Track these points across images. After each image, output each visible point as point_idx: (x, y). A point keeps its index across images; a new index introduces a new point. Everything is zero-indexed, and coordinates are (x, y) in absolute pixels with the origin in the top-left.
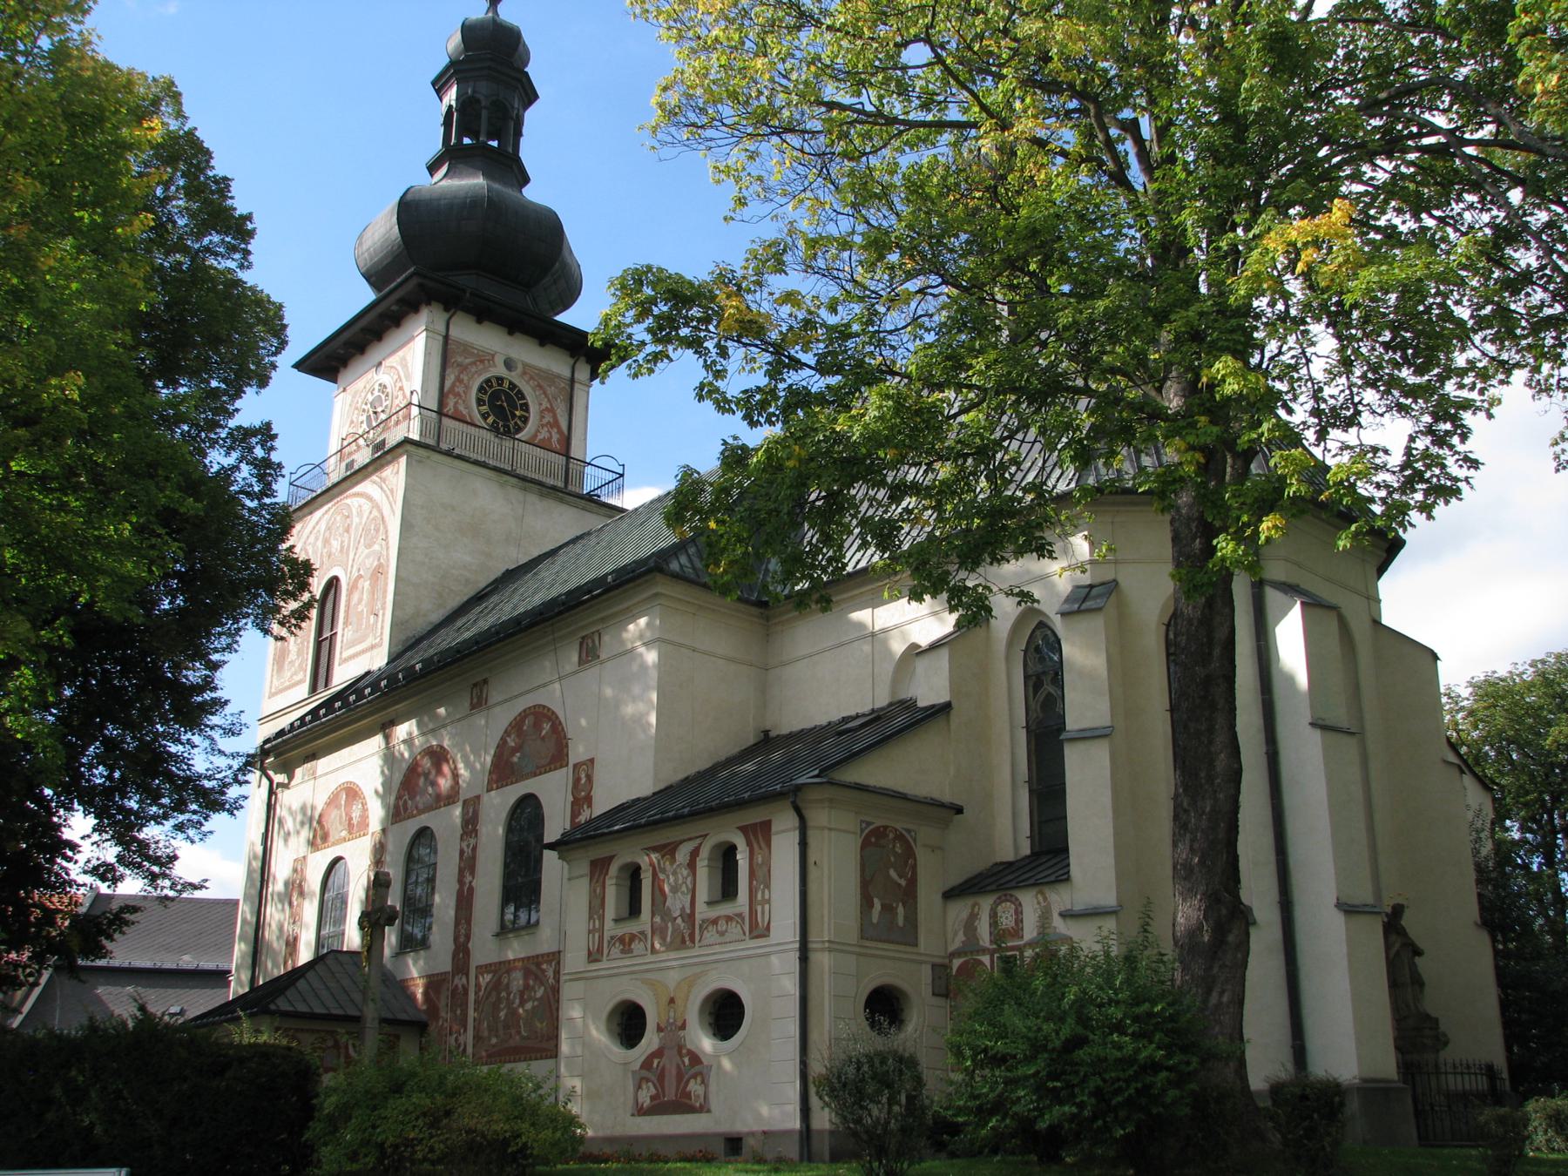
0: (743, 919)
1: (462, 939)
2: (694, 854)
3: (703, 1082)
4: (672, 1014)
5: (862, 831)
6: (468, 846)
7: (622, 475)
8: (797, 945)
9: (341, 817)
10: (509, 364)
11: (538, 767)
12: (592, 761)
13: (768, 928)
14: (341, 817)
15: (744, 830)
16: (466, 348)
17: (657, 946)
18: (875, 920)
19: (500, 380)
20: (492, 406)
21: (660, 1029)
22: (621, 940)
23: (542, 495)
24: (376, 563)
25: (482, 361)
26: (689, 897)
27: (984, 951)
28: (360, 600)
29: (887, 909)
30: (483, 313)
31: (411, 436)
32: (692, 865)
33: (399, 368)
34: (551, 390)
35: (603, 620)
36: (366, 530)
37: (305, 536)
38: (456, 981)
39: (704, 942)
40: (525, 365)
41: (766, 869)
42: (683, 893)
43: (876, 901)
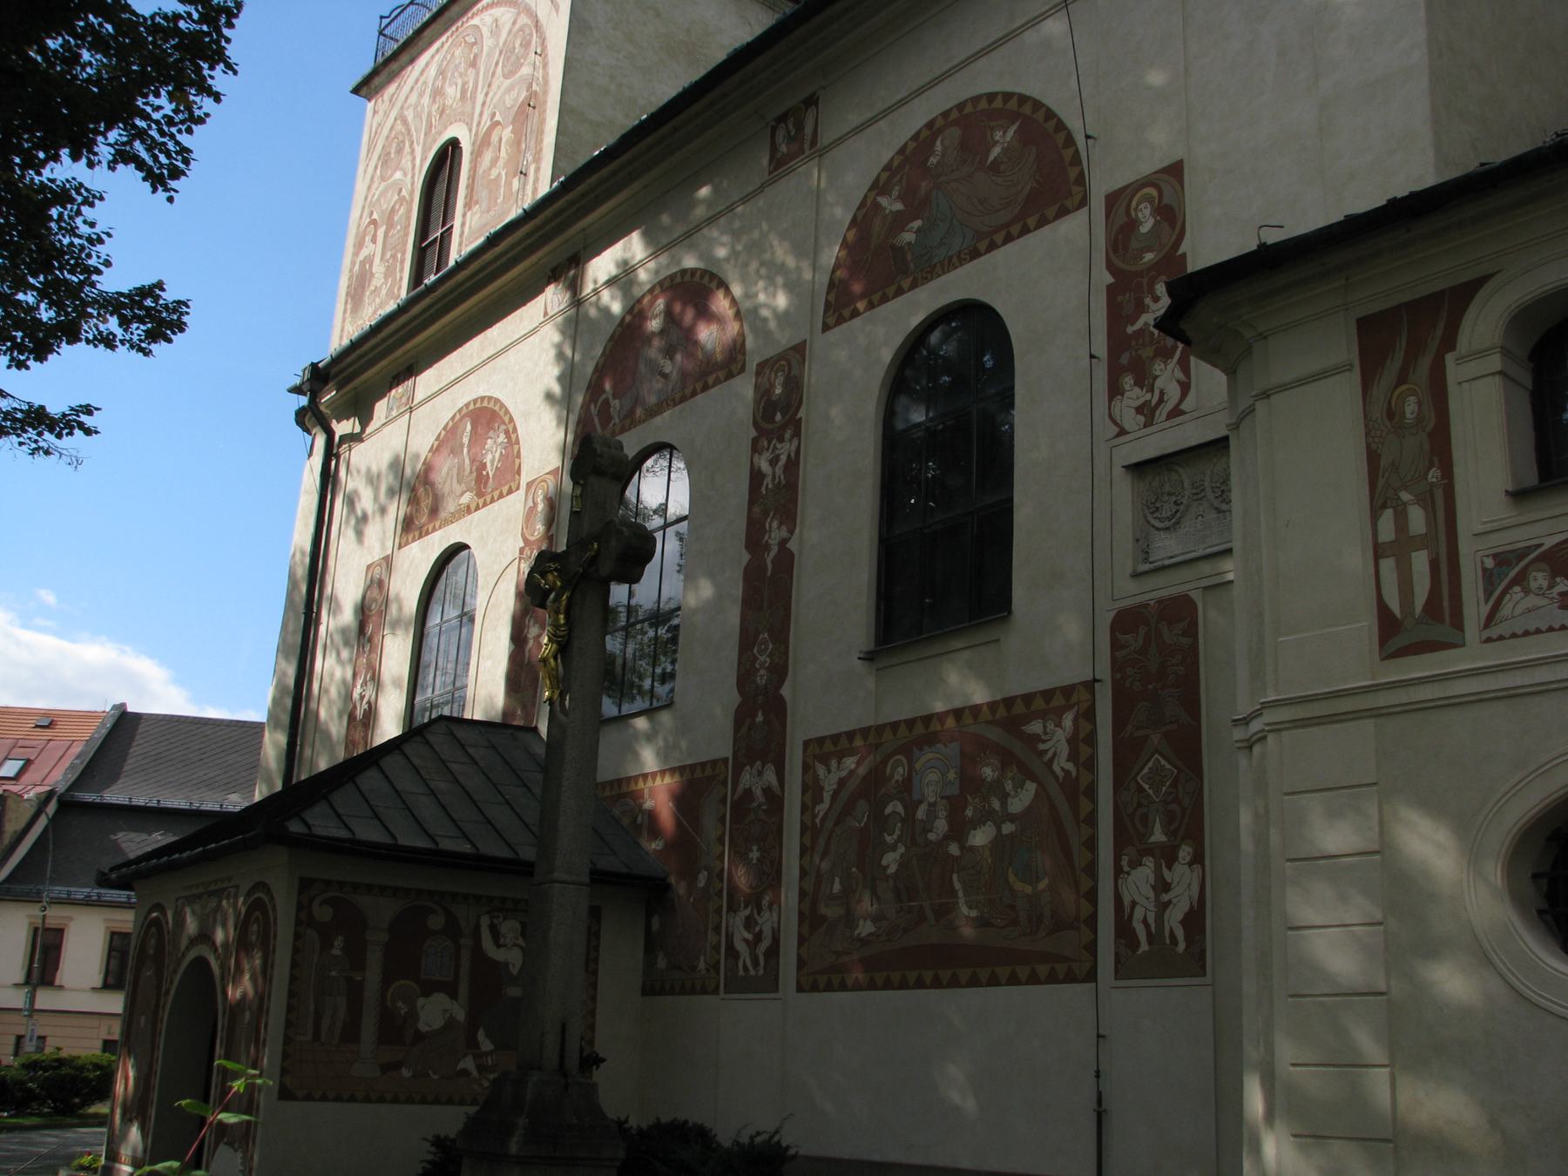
1: (762, 678)
6: (773, 462)
9: (461, 468)
14: (461, 468)
24: (524, 94)
36: (507, 51)
37: (402, 98)
38: (747, 778)
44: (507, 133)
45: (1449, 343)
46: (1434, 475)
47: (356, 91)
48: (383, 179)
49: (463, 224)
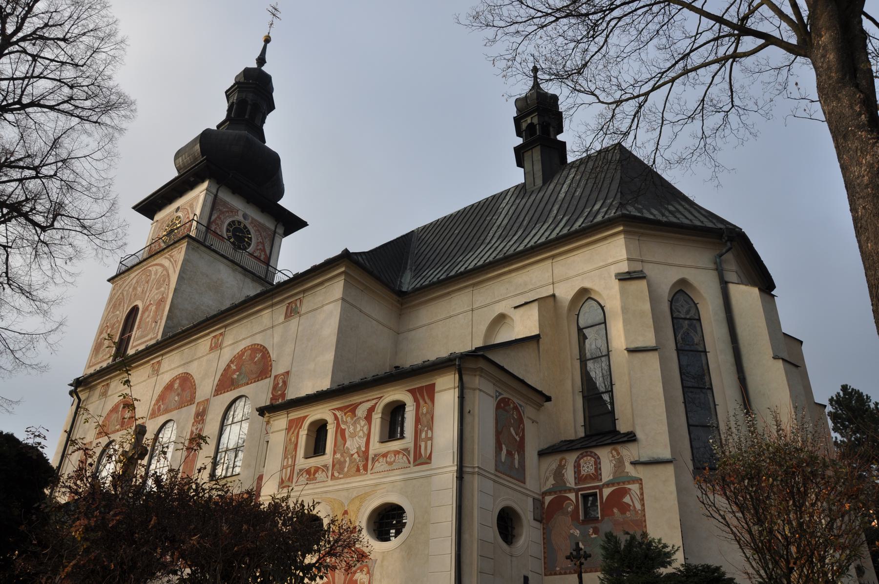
0: (409, 452)
2: (371, 410)
3: (368, 572)
5: (497, 398)
6: (197, 429)
8: (455, 468)
9: (118, 417)
10: (245, 216)
11: (249, 380)
13: (430, 457)
14: (118, 417)
15: (412, 392)
16: (225, 204)
17: (336, 474)
18: (503, 460)
19: (239, 223)
20: (234, 235)
22: (308, 472)
23: (253, 280)
25: (232, 212)
26: (365, 439)
27: (570, 490)
28: (149, 316)
29: (509, 453)
30: (236, 190)
31: (191, 234)
32: (368, 418)
33: (189, 208)
34: (264, 234)
35: (304, 291)
36: (158, 281)
37: (123, 287)
40: (253, 219)
41: (429, 416)
42: (360, 437)
43: (504, 446)
44: (154, 308)
45: (301, 428)
46: (294, 452)
47: (109, 280)
48: (113, 312)
49: (136, 334)
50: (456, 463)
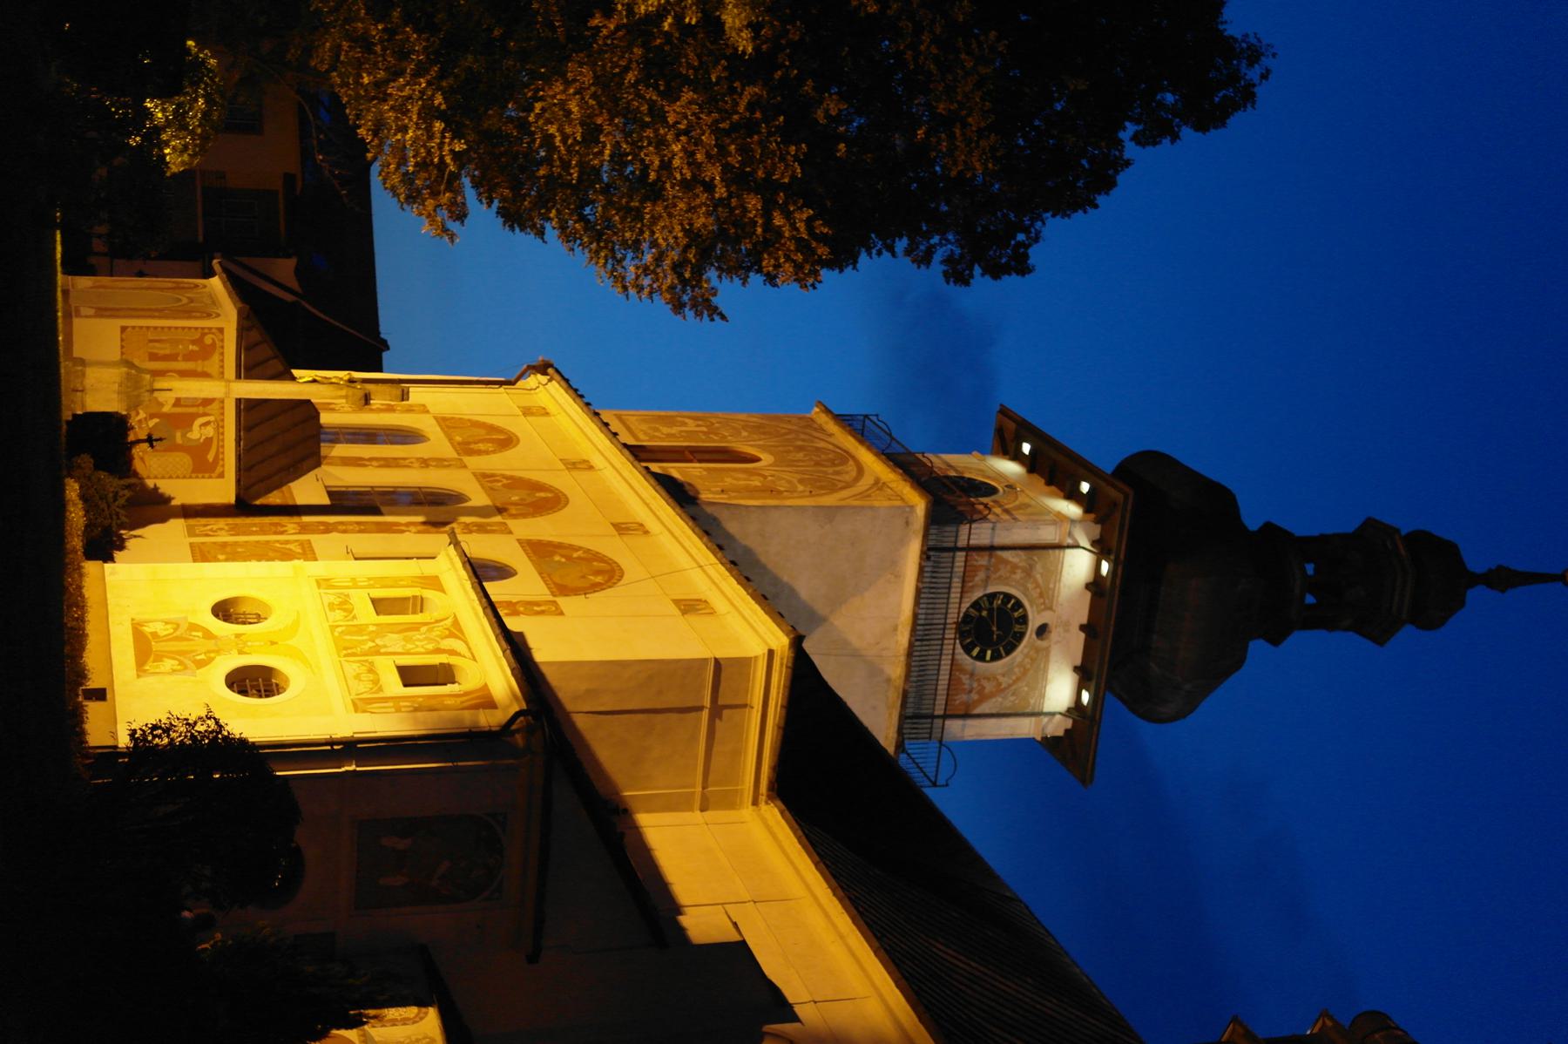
1: (340, 527)
3: (174, 671)
4: (257, 643)
7: (935, 784)
12: (561, 613)
17: (340, 629)
19: (1024, 620)
21: (238, 636)
39: (346, 665)
50: (356, 736)
